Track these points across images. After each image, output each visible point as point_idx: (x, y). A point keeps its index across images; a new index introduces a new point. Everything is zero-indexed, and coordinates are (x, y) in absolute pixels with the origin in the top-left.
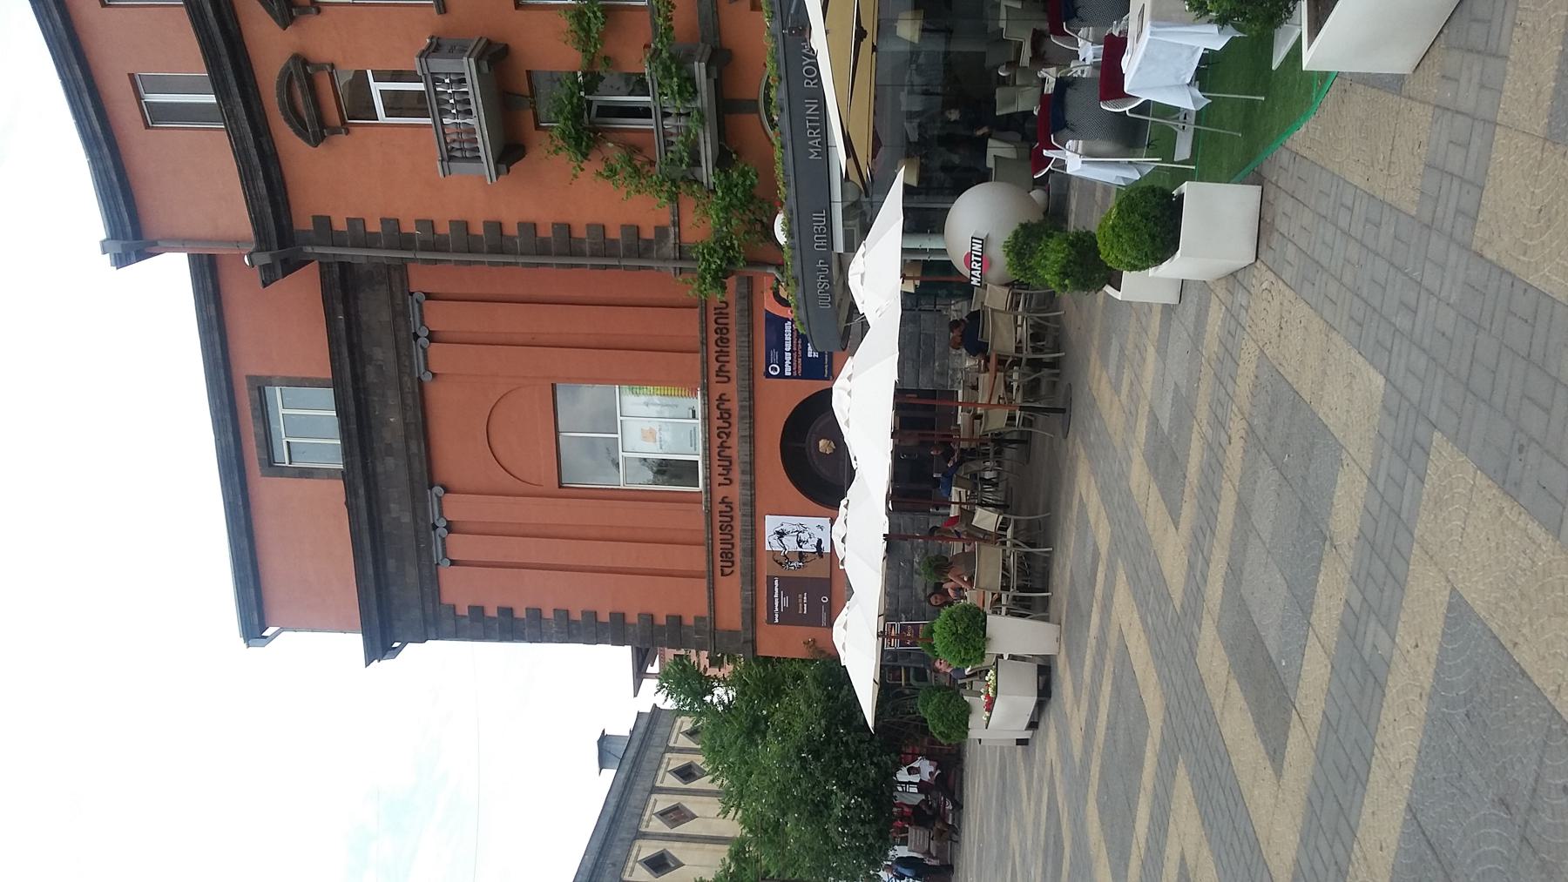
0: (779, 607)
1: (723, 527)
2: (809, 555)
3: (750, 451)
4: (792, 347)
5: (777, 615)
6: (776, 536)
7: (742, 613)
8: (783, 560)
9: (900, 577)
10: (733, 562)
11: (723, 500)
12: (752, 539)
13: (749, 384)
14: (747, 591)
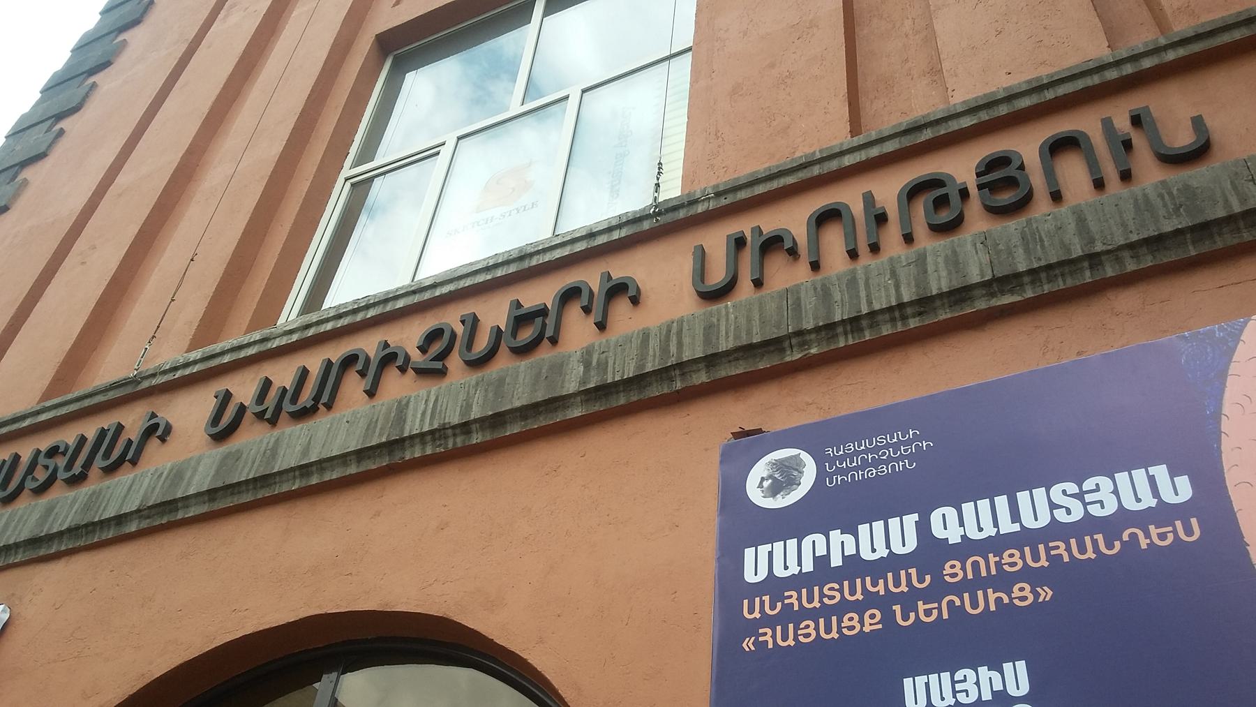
3: (323, 464)
4: (967, 547)
13: (682, 367)
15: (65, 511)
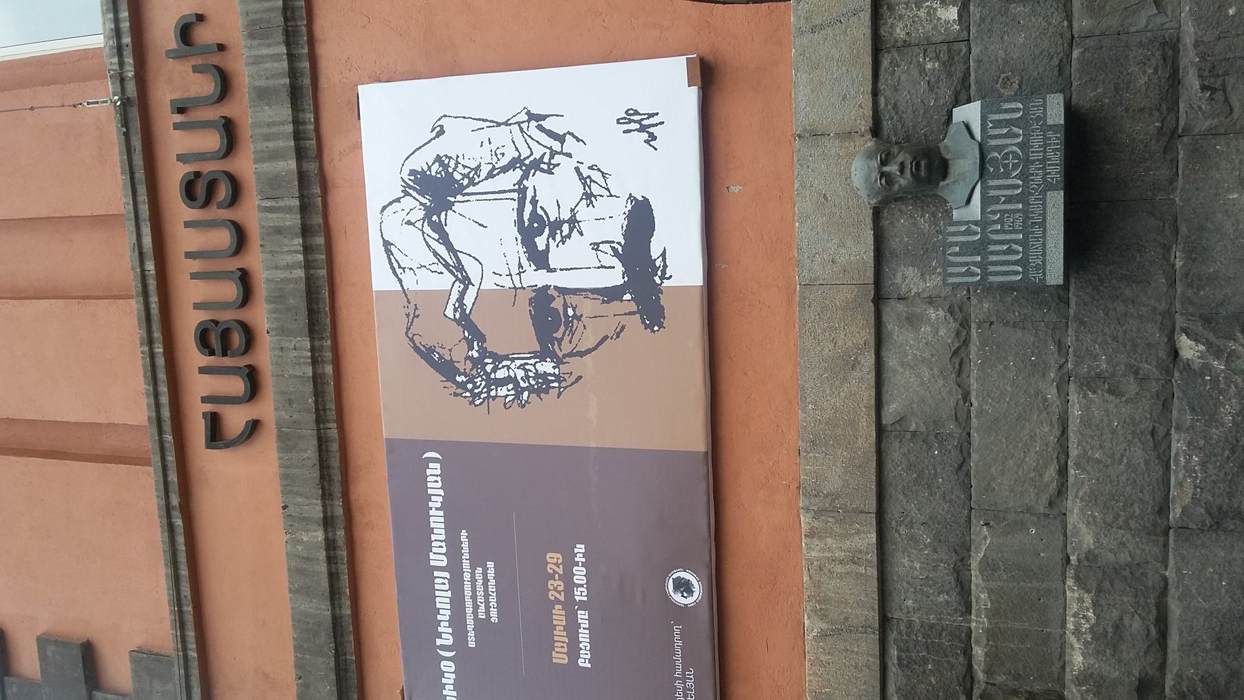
0: (457, 621)
1: (200, 189)
2: (587, 307)
5: (448, 667)
6: (414, 206)
7: (299, 648)
8: (459, 354)
9: (1178, 444)
10: (252, 377)
11: (185, 32)
12: (306, 231)
14: (304, 520)
15: (268, 65)
